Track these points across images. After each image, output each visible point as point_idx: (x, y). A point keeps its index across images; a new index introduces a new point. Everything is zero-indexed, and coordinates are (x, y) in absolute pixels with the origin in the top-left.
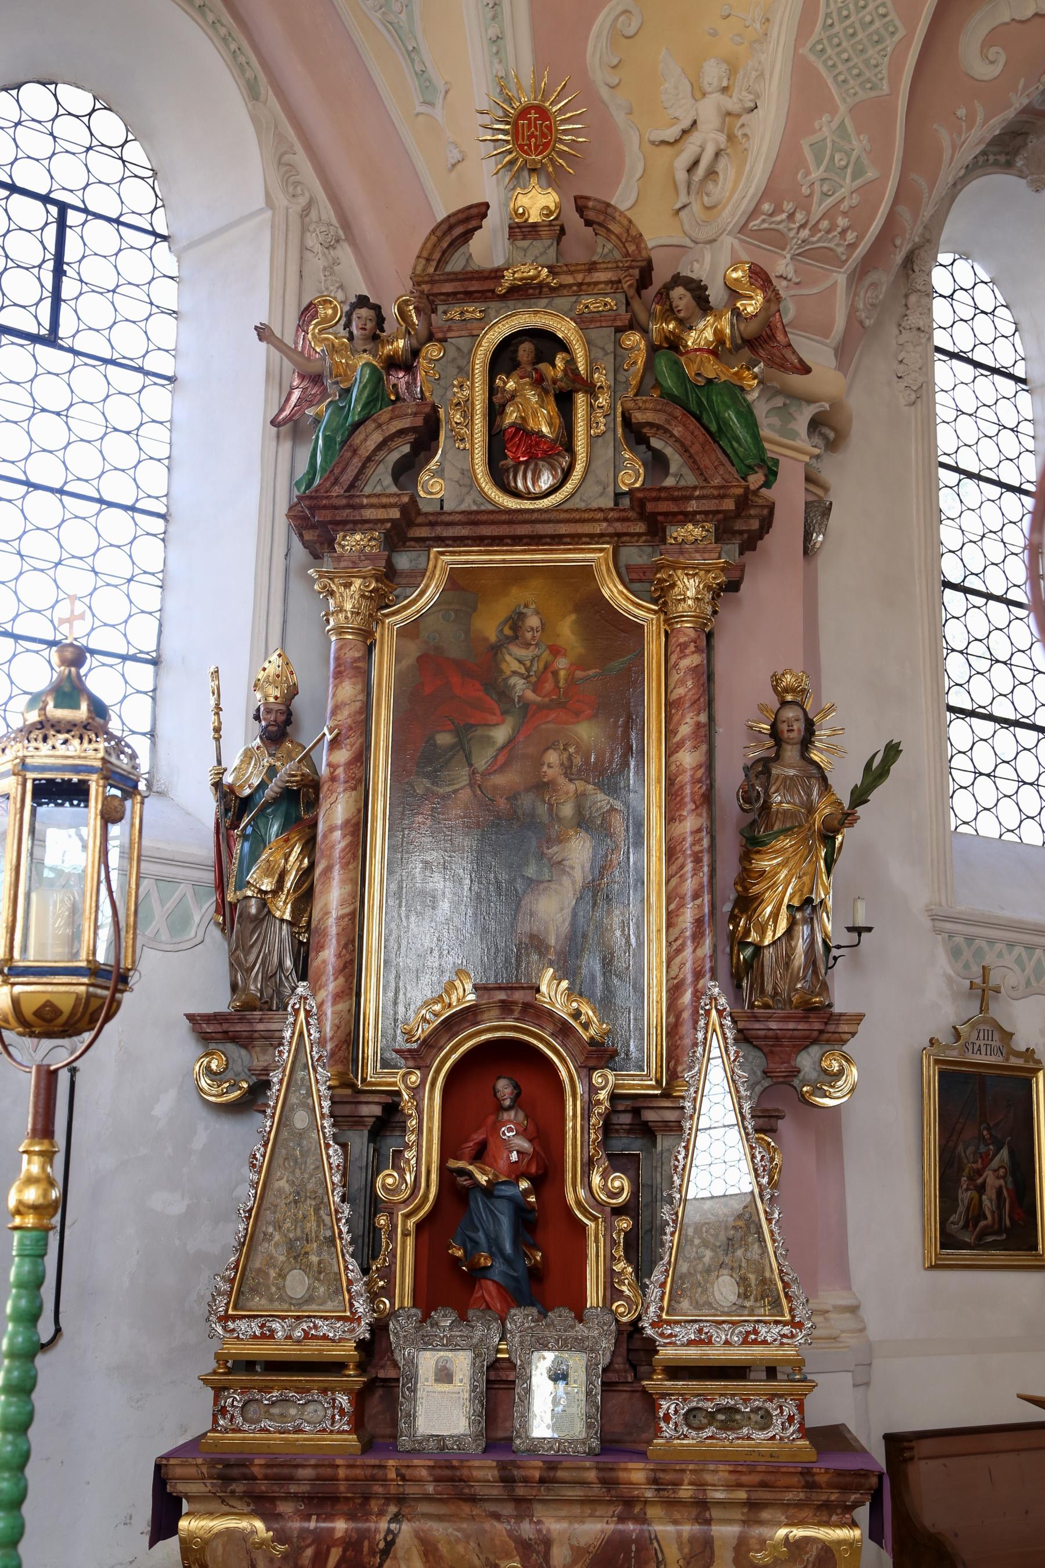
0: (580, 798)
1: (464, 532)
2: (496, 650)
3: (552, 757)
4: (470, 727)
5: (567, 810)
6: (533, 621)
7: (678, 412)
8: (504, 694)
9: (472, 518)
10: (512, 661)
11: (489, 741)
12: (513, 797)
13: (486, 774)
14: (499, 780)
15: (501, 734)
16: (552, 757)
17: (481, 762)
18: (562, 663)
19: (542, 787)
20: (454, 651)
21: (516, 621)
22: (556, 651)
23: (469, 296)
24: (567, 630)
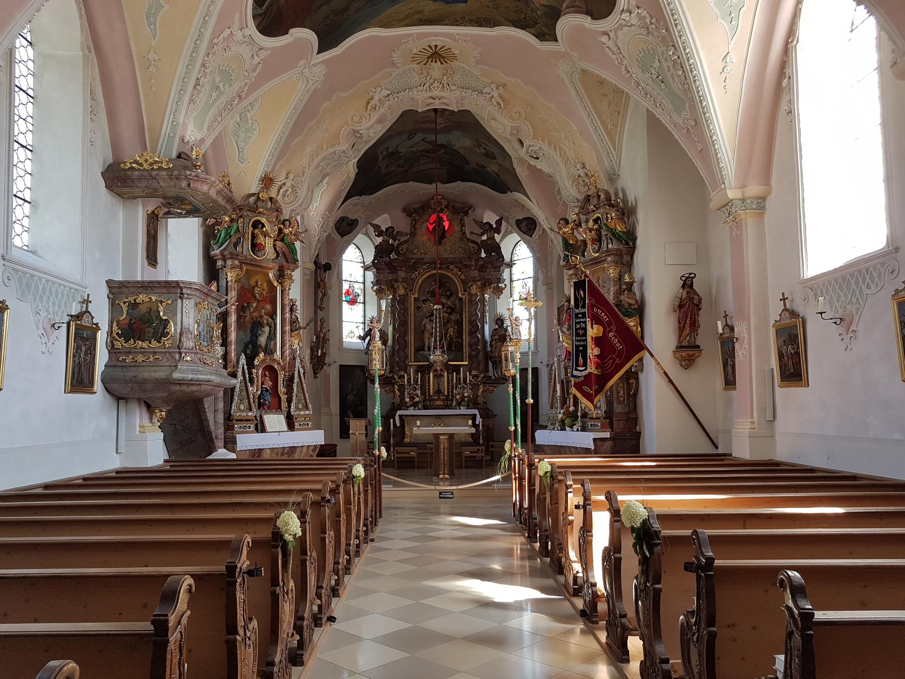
0: (267, 319)
1: (249, 262)
2: (254, 287)
3: (263, 311)
4: (250, 303)
5: (265, 322)
6: (260, 283)
7: (285, 246)
8: (255, 297)
9: (251, 260)
10: (257, 290)
11: (252, 306)
12: (256, 318)
13: (252, 313)
14: (254, 314)
15: (255, 305)
16: (263, 311)
17: (251, 310)
18: (264, 292)
19: (261, 316)
20: (247, 287)
21: (257, 282)
22: (263, 290)
23: (250, 211)
24: (265, 285)
